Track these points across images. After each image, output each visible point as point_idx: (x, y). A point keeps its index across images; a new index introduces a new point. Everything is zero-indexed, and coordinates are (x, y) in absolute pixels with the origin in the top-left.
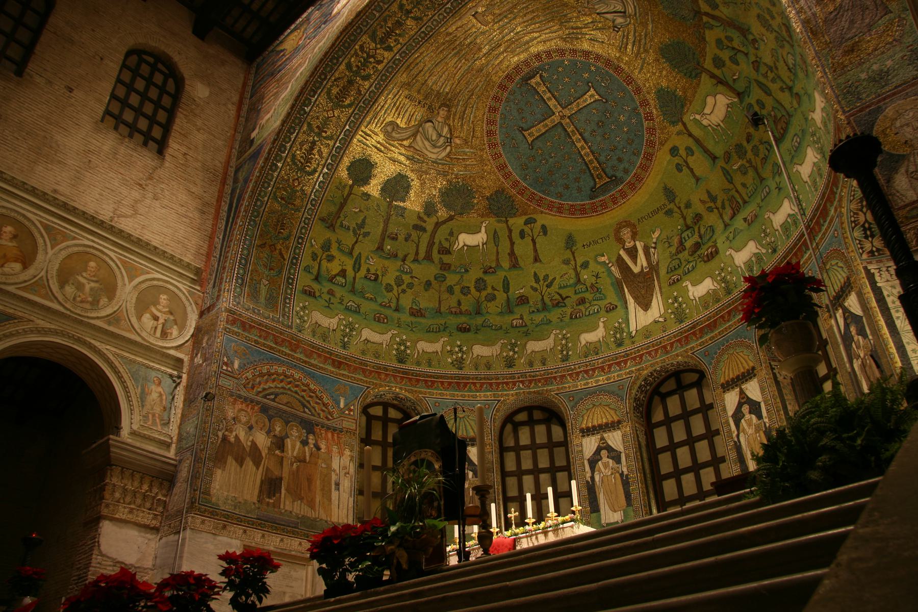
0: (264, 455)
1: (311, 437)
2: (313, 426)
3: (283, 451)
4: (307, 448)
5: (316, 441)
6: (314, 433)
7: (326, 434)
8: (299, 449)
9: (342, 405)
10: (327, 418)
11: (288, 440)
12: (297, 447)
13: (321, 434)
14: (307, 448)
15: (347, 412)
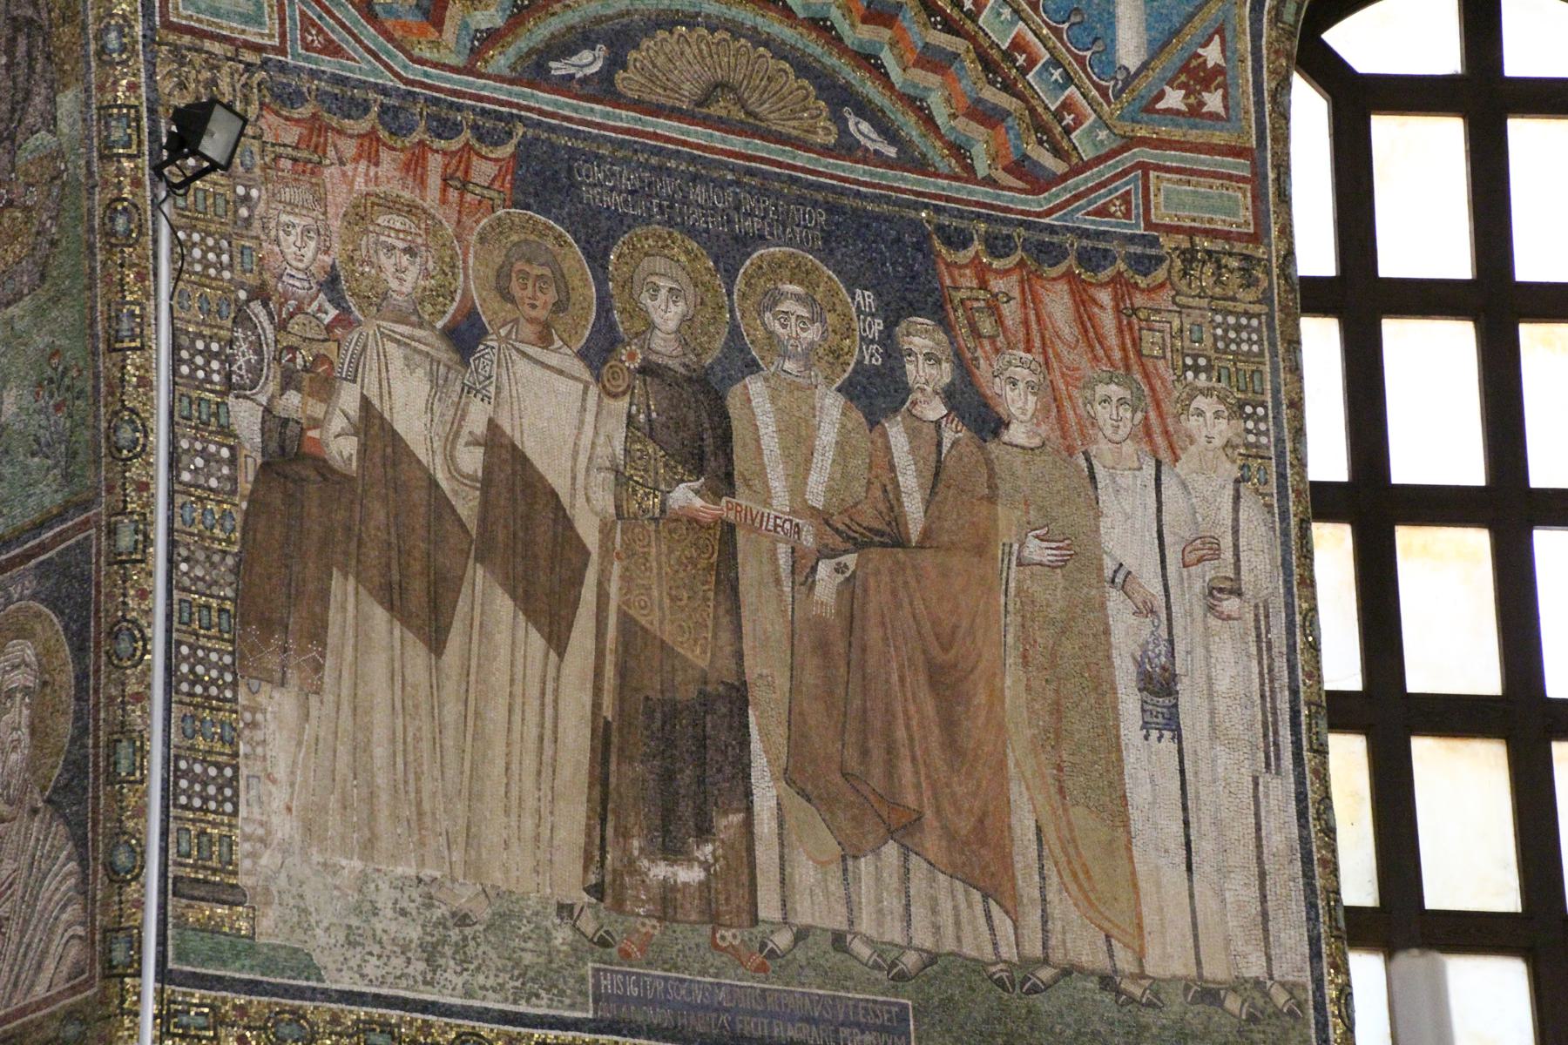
0: (588, 529)
1: (920, 337)
2: (923, 245)
3: (724, 483)
4: (897, 433)
5: (964, 368)
6: (939, 311)
7: (1030, 299)
8: (843, 447)
9: (1129, 48)
10: (1021, 168)
11: (755, 386)
12: (827, 436)
13: (993, 309)
14: (897, 433)
15: (1174, 99)
